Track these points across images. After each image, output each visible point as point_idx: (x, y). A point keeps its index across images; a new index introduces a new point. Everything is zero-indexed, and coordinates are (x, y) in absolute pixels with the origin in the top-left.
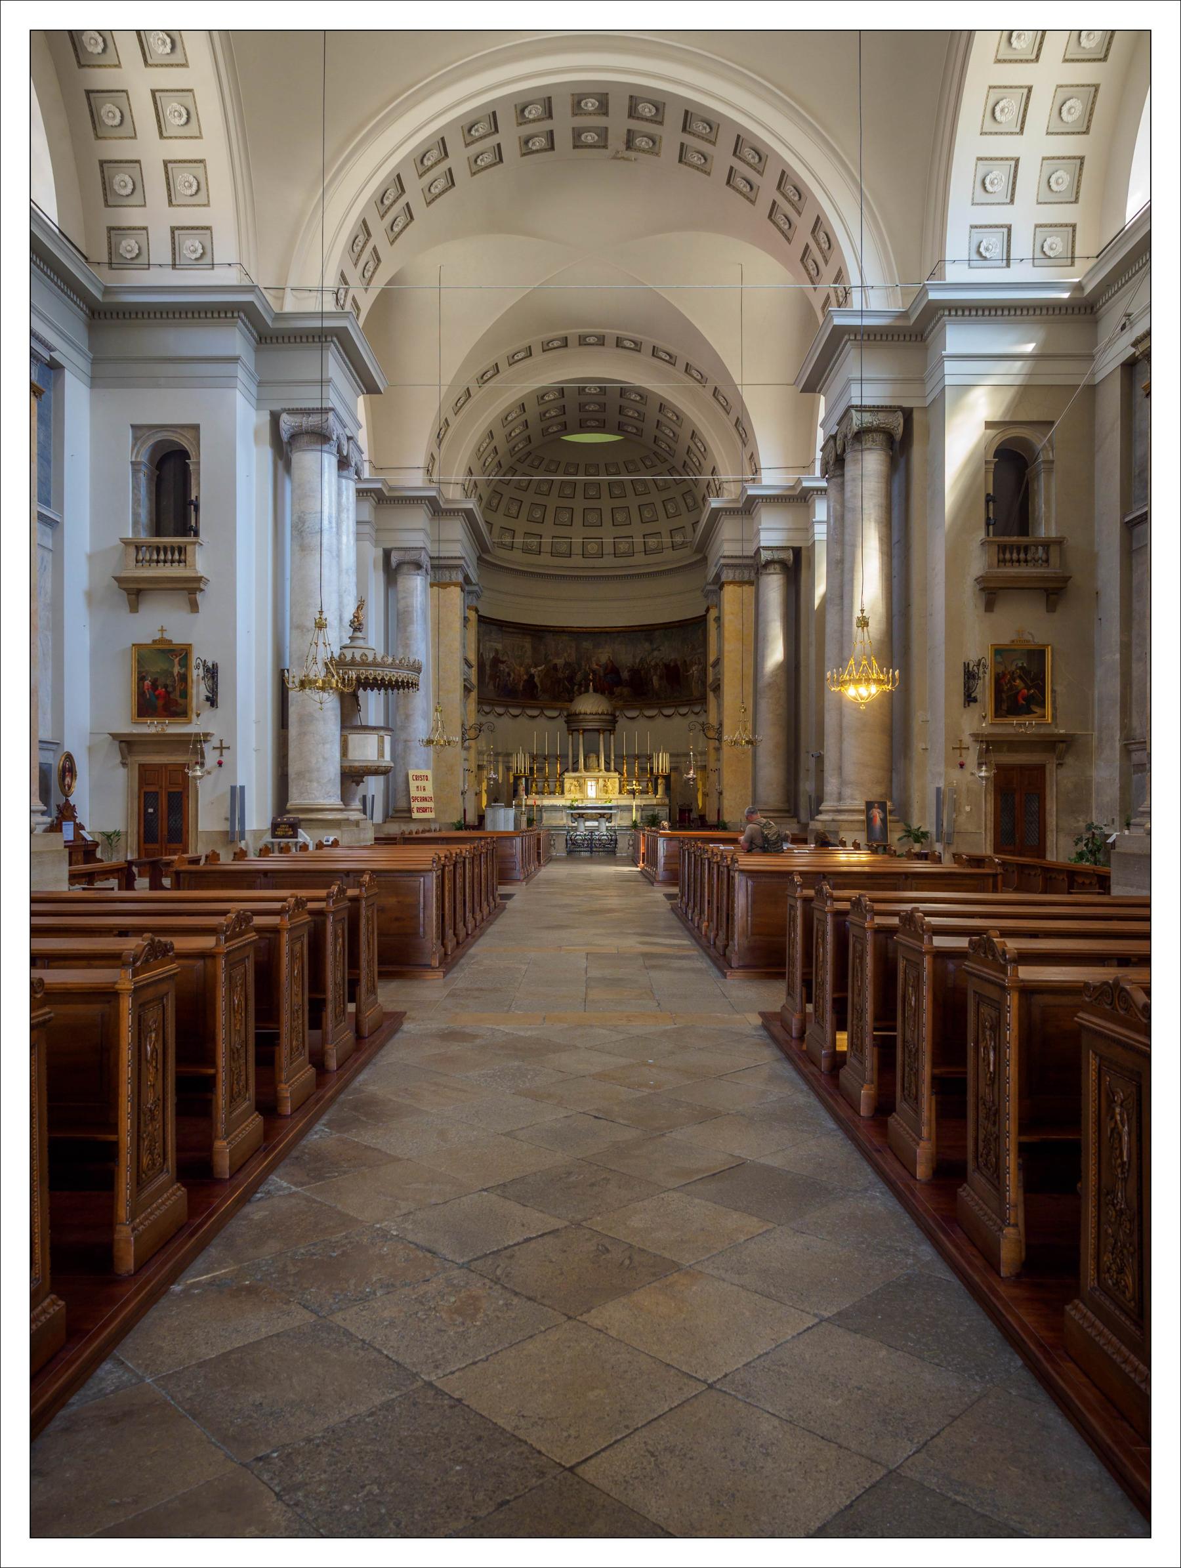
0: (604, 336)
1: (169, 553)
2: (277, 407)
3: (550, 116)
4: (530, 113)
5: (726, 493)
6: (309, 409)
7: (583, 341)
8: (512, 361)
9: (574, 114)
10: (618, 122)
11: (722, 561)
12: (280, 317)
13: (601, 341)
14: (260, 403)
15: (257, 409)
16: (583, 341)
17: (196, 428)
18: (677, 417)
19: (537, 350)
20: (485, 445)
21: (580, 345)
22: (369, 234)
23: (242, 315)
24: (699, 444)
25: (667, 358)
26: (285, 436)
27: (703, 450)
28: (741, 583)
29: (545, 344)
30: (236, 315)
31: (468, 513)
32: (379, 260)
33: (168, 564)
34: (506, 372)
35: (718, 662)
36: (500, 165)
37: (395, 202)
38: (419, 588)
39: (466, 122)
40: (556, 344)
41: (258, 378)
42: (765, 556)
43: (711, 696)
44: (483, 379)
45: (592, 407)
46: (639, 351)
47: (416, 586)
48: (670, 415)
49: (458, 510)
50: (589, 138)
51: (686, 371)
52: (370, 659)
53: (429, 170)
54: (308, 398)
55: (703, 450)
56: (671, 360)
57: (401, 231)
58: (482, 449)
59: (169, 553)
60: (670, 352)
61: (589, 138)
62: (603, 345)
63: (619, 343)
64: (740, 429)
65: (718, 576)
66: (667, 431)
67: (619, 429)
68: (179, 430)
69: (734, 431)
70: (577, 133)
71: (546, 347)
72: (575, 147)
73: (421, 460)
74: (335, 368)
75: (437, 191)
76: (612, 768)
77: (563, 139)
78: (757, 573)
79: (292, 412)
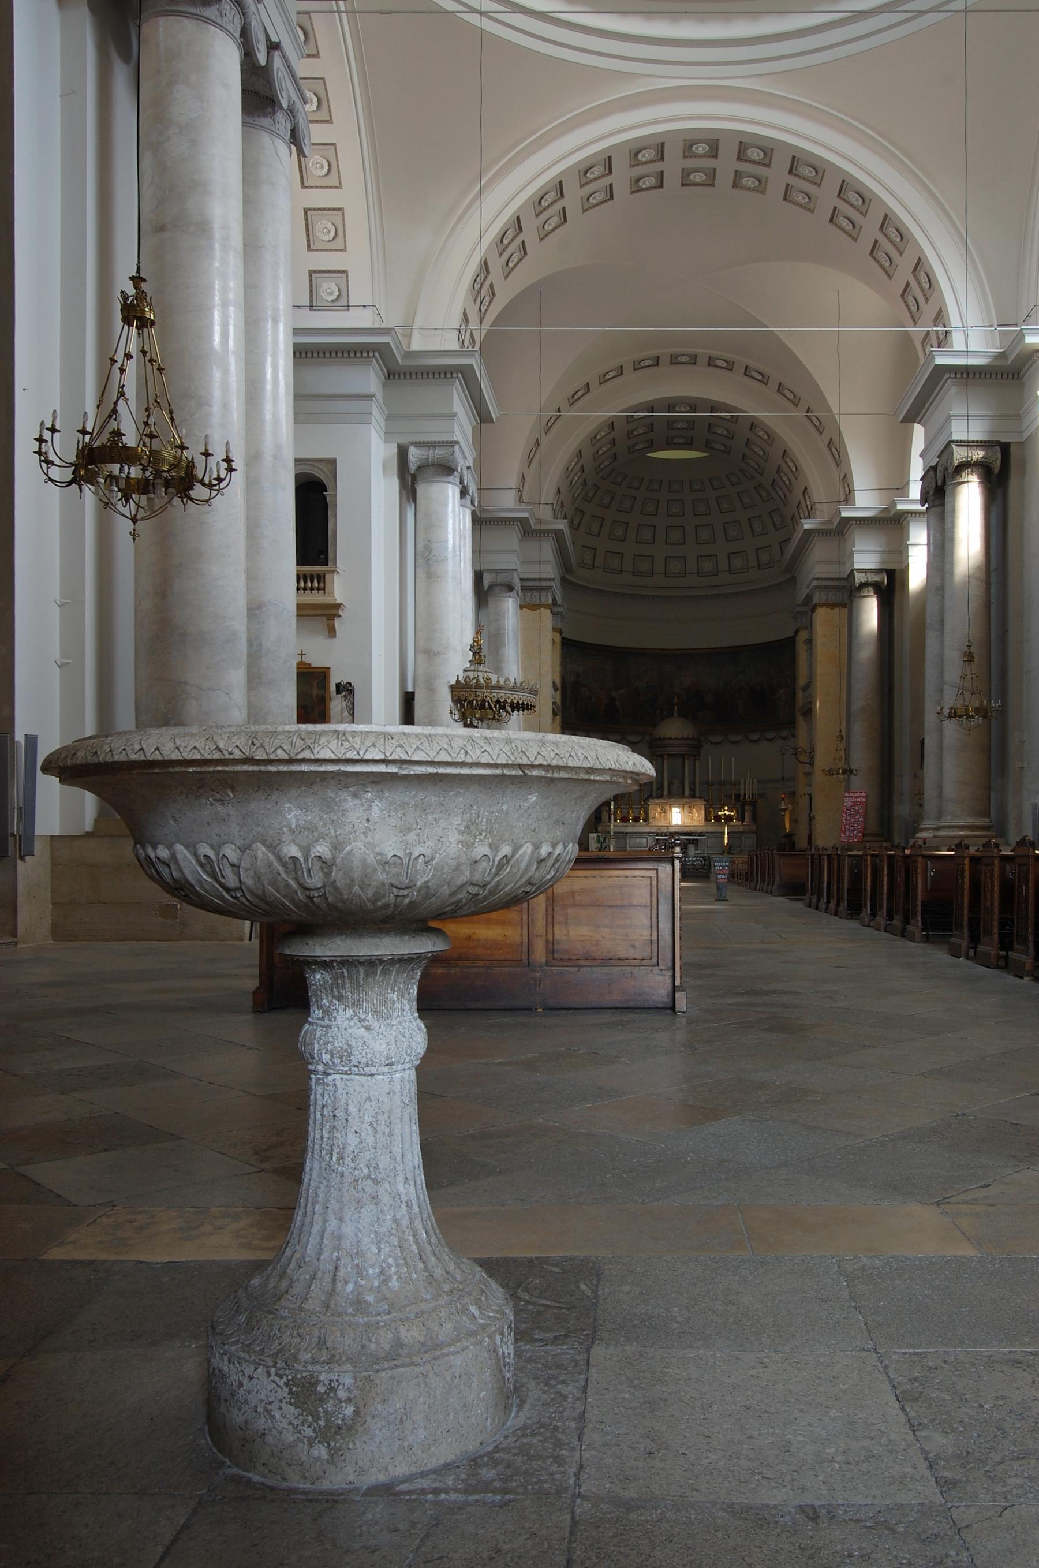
0: (696, 356)
1: (309, 581)
2: (404, 440)
3: (662, 159)
4: (643, 156)
5: (818, 513)
6: (435, 442)
7: (674, 360)
8: (603, 380)
9: (685, 157)
10: (726, 165)
11: (815, 583)
12: (410, 354)
13: (693, 360)
14: (388, 435)
15: (385, 442)
16: (674, 360)
17: (332, 462)
18: (769, 436)
19: (628, 369)
20: (573, 464)
21: (671, 363)
22: (488, 272)
23: (377, 354)
24: (791, 464)
25: (760, 377)
26: (412, 468)
27: (794, 469)
28: (832, 606)
29: (636, 363)
30: (371, 354)
31: (558, 534)
32: (494, 294)
33: (315, 591)
34: (596, 391)
35: (808, 686)
36: (611, 202)
37: (512, 240)
38: (511, 610)
39: (584, 167)
40: (647, 363)
41: (387, 413)
42: (859, 578)
43: (800, 720)
44: (573, 400)
45: (680, 425)
46: (731, 370)
47: (510, 605)
48: (761, 434)
49: (548, 532)
50: (698, 177)
51: (778, 390)
52: (494, 682)
53: (545, 209)
54: (433, 432)
55: (794, 469)
56: (764, 380)
57: (515, 266)
58: (570, 469)
59: (309, 581)
60: (761, 371)
61: (698, 177)
62: (695, 363)
63: (711, 362)
64: (834, 450)
65: (809, 597)
66: (757, 450)
67: (707, 446)
68: (317, 464)
69: (826, 451)
70: (686, 173)
71: (637, 367)
72: (683, 185)
73: (513, 482)
74: (459, 403)
75: (550, 228)
76: (697, 795)
77: (672, 179)
78: (851, 595)
79: (418, 445)
